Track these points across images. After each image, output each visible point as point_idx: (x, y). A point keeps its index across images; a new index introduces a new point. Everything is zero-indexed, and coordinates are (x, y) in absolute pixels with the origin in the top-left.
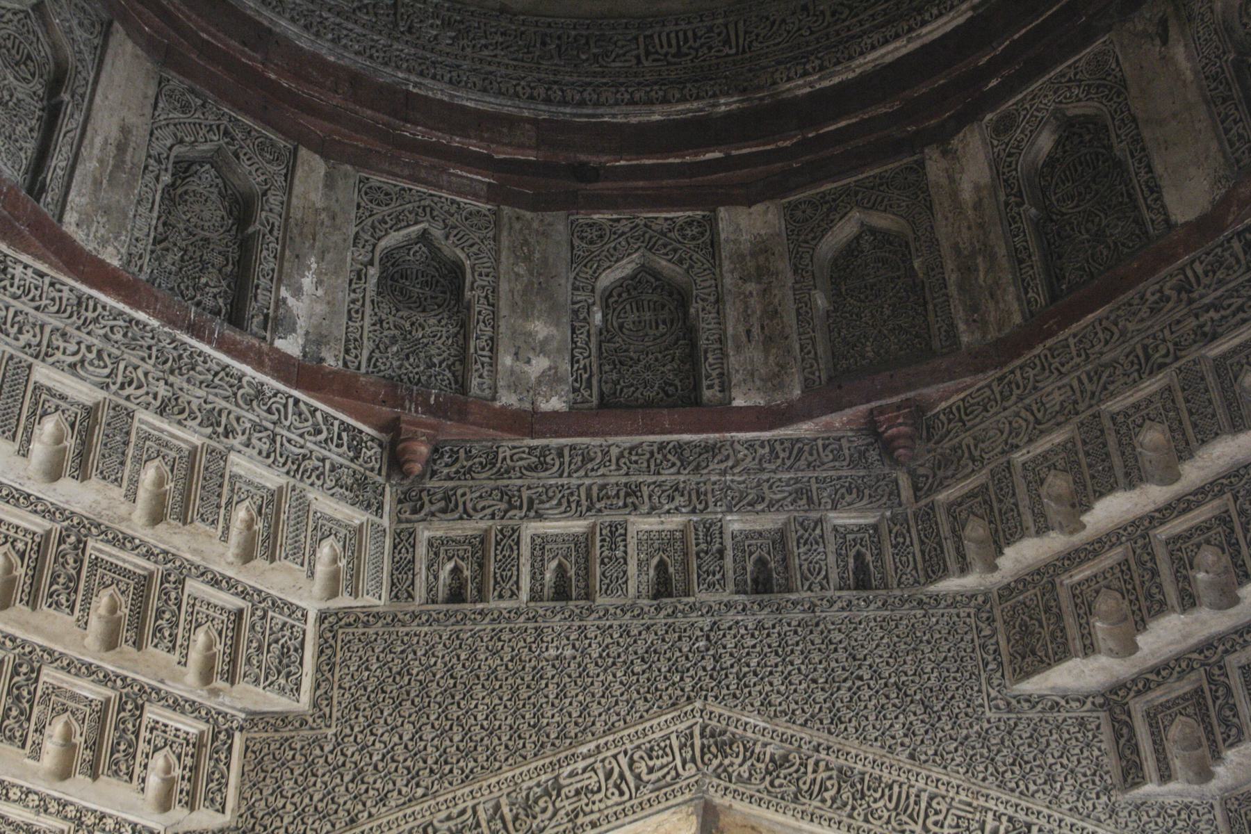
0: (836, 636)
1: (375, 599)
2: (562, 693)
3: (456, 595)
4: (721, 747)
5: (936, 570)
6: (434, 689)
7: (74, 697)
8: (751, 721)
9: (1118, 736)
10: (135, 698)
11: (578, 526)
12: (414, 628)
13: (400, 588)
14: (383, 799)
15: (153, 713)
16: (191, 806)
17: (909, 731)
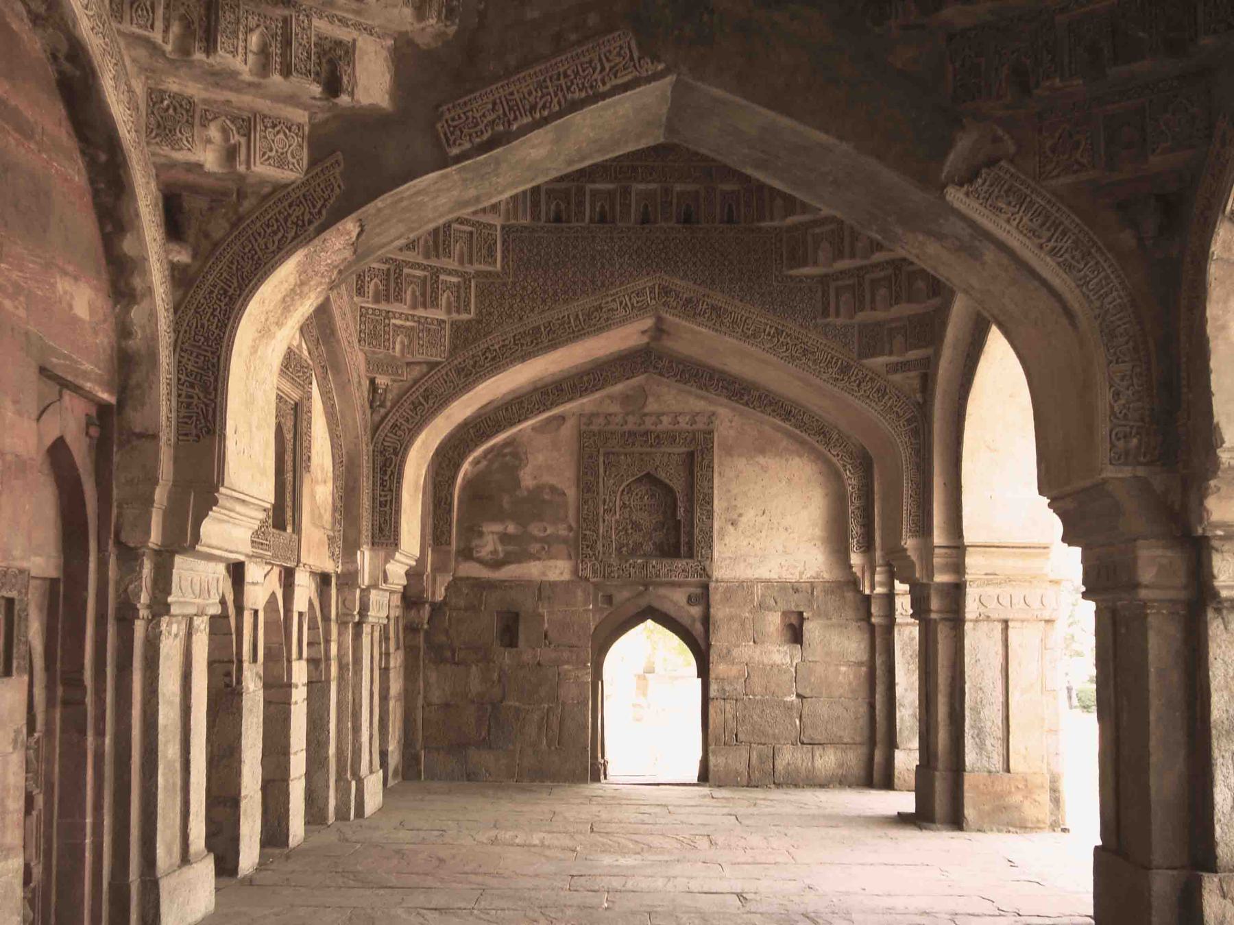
0: (716, 245)
1: (526, 221)
2: (603, 266)
3: (558, 219)
4: (666, 293)
5: (762, 218)
6: (551, 263)
7: (414, 276)
8: (678, 283)
9: (823, 295)
10: (436, 272)
11: (611, 186)
12: (541, 234)
13: (535, 216)
14: (532, 310)
15: (442, 277)
16: (458, 312)
17: (741, 289)
